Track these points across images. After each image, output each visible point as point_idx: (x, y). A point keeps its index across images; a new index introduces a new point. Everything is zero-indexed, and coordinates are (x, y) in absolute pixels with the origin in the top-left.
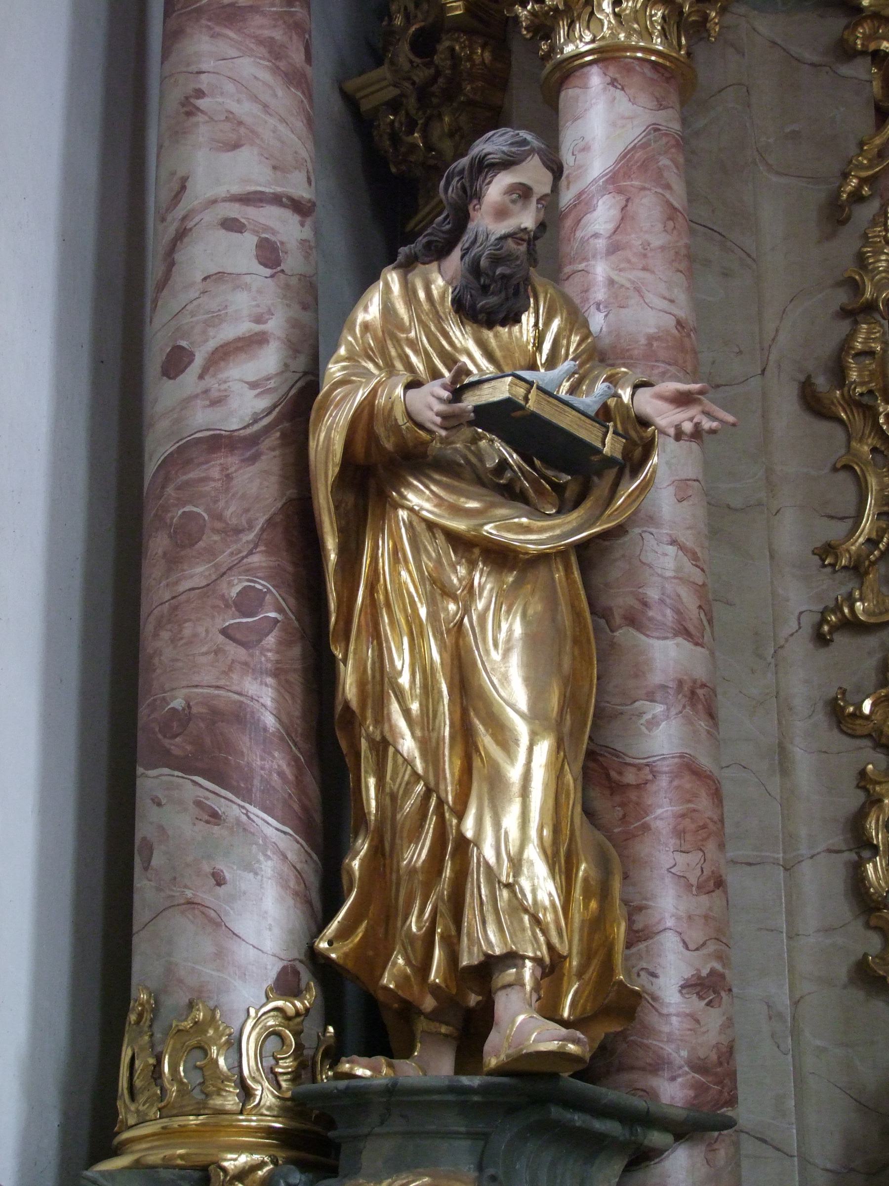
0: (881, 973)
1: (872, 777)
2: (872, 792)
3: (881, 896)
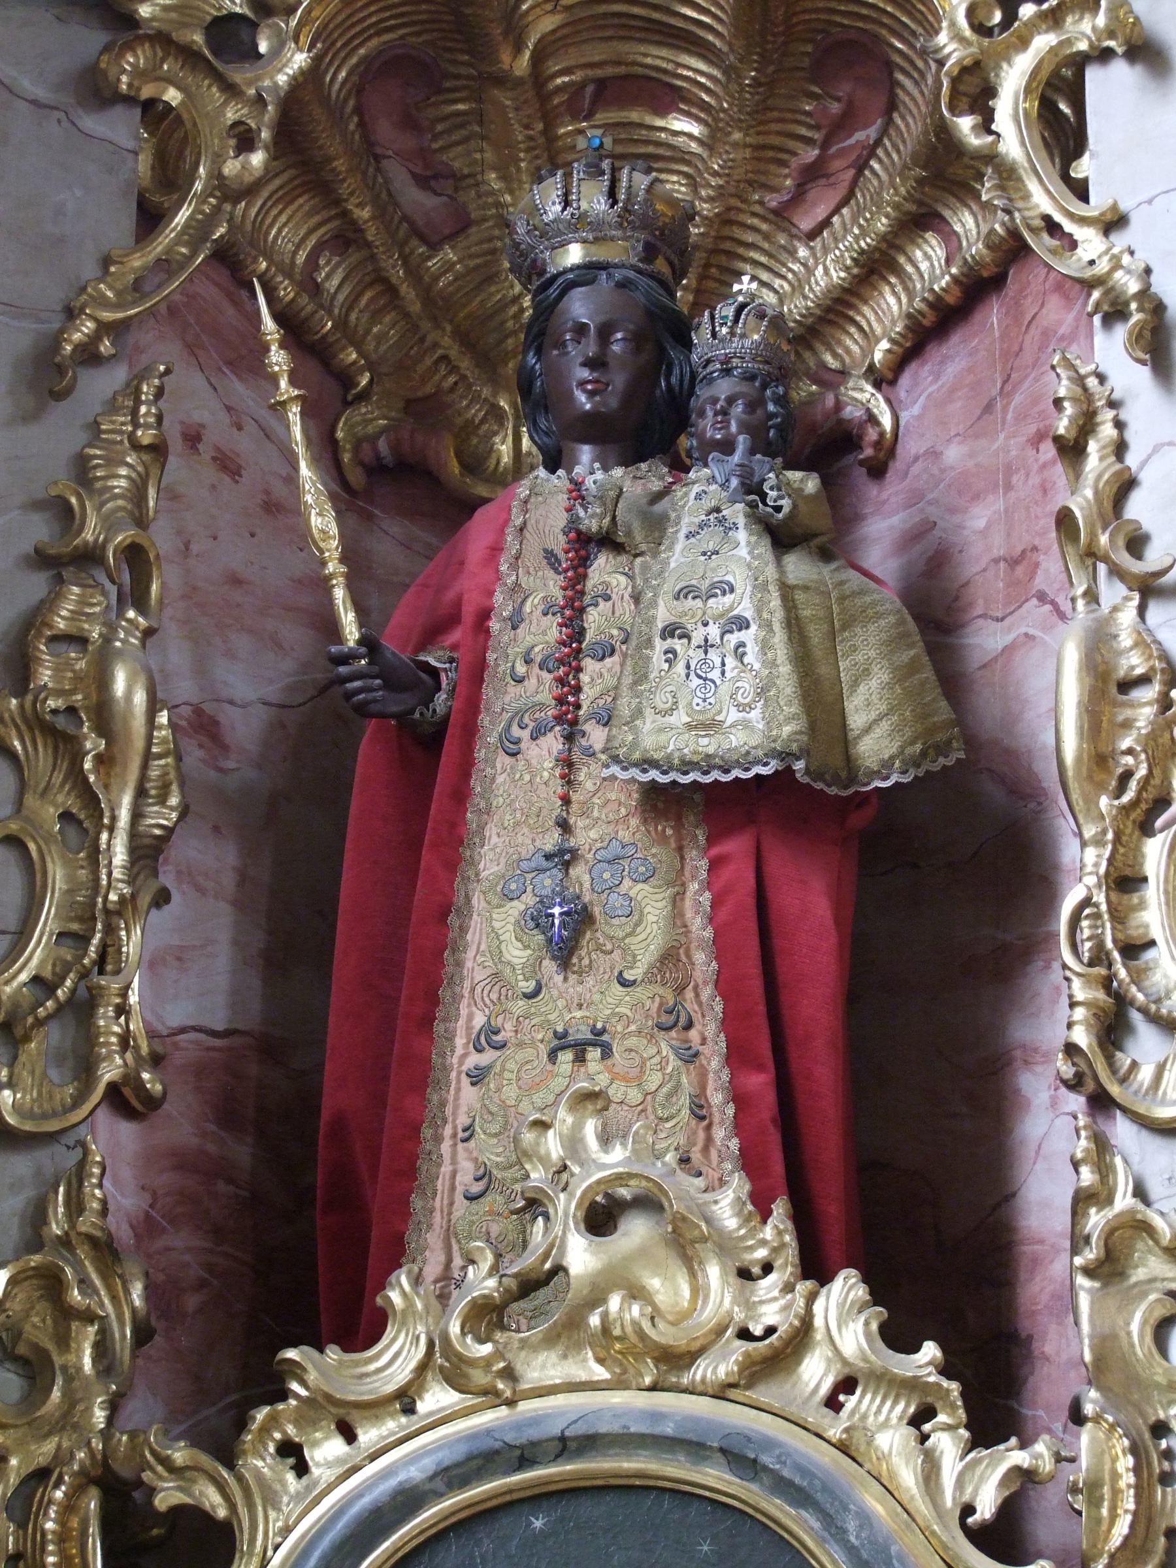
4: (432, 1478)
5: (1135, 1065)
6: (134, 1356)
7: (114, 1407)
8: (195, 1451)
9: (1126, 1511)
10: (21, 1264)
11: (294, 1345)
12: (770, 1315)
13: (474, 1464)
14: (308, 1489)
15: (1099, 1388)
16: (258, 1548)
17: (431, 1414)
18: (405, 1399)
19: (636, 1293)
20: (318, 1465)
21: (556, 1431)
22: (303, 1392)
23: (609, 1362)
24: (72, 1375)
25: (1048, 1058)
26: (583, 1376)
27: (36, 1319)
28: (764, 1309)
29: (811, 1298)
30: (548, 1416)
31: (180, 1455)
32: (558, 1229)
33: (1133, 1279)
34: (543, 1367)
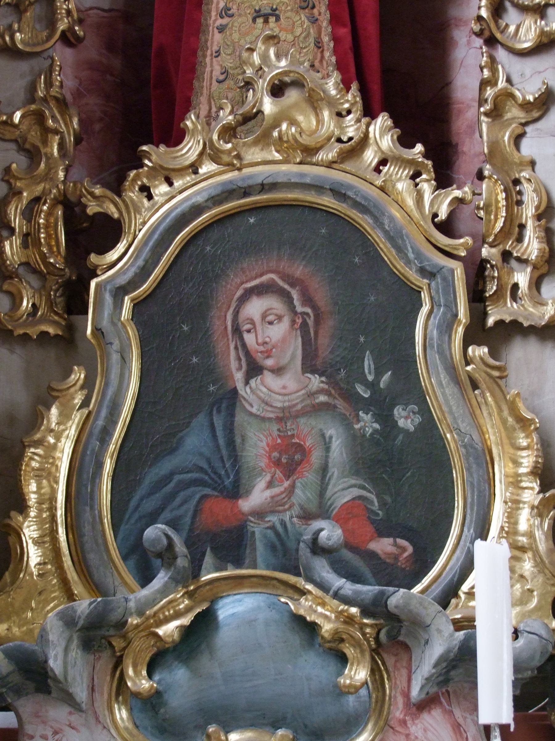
0: (10, 327)
1: (16, 174)
2: (13, 185)
3: (14, 267)
4: (207, 201)
5: (507, 26)
6: (75, 149)
7: (67, 170)
8: (105, 190)
9: (502, 217)
10: (26, 109)
11: (146, 144)
12: (351, 132)
13: (224, 195)
14: (153, 206)
15: (491, 164)
16: (132, 231)
17: (205, 174)
18: (194, 168)
19: (293, 122)
20: (157, 195)
21: (260, 181)
22: (150, 164)
23: (282, 152)
24: (49, 157)
25: (466, 23)
26: (270, 158)
27: (33, 133)
28: (348, 129)
29: (368, 125)
30: (255, 175)
31: (98, 191)
32: (259, 95)
33: (506, 118)
34: (253, 154)
